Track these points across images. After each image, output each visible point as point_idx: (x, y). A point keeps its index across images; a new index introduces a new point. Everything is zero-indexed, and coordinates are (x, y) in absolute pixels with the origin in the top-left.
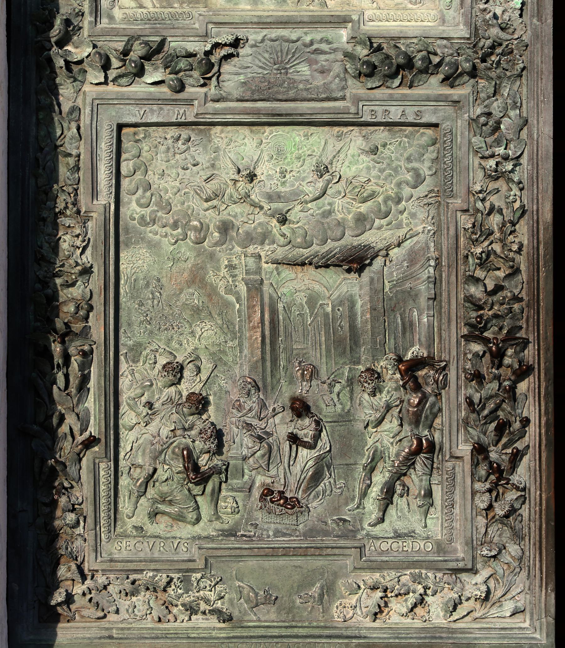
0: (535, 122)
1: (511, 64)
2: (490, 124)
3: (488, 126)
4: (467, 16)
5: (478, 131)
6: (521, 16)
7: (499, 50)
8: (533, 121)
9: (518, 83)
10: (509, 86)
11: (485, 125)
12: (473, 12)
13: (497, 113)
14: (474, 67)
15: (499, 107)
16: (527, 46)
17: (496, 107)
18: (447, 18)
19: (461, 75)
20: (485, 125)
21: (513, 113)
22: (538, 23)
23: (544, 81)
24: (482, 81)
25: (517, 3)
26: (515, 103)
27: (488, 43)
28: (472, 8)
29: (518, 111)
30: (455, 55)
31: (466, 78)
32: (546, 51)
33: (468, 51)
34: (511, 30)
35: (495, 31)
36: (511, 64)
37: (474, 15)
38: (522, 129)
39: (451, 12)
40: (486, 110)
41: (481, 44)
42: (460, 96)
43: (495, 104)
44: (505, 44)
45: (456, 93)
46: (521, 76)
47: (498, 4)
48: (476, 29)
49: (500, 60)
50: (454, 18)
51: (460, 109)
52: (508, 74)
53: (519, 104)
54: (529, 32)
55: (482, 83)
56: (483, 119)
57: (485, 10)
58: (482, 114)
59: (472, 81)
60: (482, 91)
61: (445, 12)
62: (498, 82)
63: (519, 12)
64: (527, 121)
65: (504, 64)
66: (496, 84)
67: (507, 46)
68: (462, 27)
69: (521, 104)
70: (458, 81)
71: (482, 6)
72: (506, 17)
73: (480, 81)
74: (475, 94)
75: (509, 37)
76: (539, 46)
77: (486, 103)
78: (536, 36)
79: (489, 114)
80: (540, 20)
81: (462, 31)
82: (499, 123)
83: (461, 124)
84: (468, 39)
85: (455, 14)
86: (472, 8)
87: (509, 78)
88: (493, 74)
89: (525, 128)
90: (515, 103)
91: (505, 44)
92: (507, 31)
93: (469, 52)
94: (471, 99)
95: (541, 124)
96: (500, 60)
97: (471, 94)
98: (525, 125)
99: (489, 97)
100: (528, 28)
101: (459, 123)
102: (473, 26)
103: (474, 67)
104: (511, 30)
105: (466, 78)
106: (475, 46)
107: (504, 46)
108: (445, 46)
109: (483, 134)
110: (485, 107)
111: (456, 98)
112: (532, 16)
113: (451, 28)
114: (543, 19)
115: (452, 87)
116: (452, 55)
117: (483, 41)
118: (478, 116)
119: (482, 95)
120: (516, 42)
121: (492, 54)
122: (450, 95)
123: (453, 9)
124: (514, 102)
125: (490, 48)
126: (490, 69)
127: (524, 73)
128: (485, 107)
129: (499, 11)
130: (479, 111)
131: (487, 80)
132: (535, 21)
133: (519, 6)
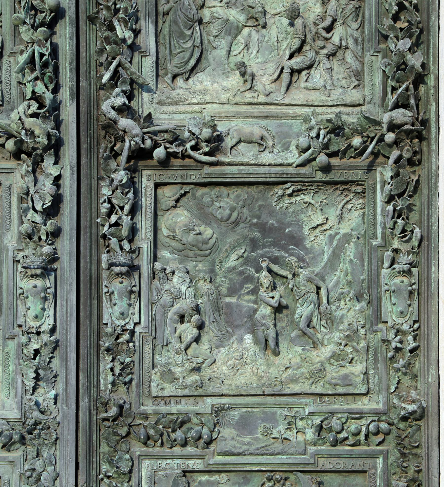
0: (64, 474)
1: (48, 436)
2: (34, 476)
3: (32, 478)
4: (18, 403)
5: (26, 481)
6: (55, 403)
7: (40, 427)
8: (62, 474)
9: (54, 448)
10: (47, 451)
11: (31, 476)
12: (23, 400)
13: (39, 468)
14: (23, 438)
15: (40, 465)
16: (59, 424)
17: (38, 465)
18: (6, 405)
19: (14, 443)
20: (31, 476)
21: (50, 469)
22: (66, 408)
23: (69, 447)
24: (29, 447)
25: (51, 395)
26: (51, 462)
27: (32, 422)
28: (22, 398)
29: (53, 468)
30: (10, 429)
31: (18, 445)
32: (71, 427)
33: (19, 427)
34: (49, 413)
35: (36, 414)
36: (48, 436)
37: (24, 403)
38: (56, 479)
39: (9, 401)
40: (32, 467)
41: (27, 422)
42: (14, 457)
43: (38, 463)
44: (43, 422)
45: (11, 455)
46: (56, 444)
47: (41, 395)
48: (25, 413)
49: (40, 433)
50: (11, 405)
51: (14, 466)
52: (46, 442)
53: (54, 463)
54: (60, 414)
55: (30, 448)
56: (28, 473)
57: (30, 399)
58: (28, 469)
59: (23, 447)
60: (29, 454)
61: (5, 401)
62: (39, 448)
63: (54, 401)
64: (59, 474)
65: (43, 436)
66: (38, 449)
67: (45, 423)
68: (16, 411)
69: (56, 462)
70: (13, 447)
71: (29, 397)
72: (45, 404)
73: (28, 447)
74: (25, 456)
75: (46, 417)
76: (66, 423)
77: (31, 462)
78: (65, 417)
79: (34, 470)
80: (67, 406)
81: (14, 414)
82: (40, 475)
83: (15, 477)
84: (20, 419)
85: (12, 402)
86: (22, 398)
87: (47, 445)
88: (36, 442)
89: (58, 479)
90: (51, 462)
91: (43, 422)
92: (46, 414)
93: (20, 428)
94: (22, 459)
95: (67, 476)
96: (40, 433)
97: (22, 456)
98: (58, 477)
99: (34, 458)
100: (60, 411)
101: (14, 477)
102: (23, 410)
103: (23, 438)
104: (49, 413)
105: (18, 445)
106: (24, 424)
107: (43, 424)
108: (3, 424)
109: (29, 483)
110: (31, 464)
111: (11, 459)
112: (62, 404)
113: (8, 412)
114: (69, 405)
115: (9, 451)
116: (8, 430)
117: (29, 420)
118: (26, 471)
119: (29, 457)
120: (51, 420)
121: (35, 429)
122: (7, 457)
123: (10, 399)
124: (50, 461)
125: (34, 425)
126: (34, 439)
127: (58, 441)
128: (31, 464)
129: (40, 400)
130: (27, 467)
131: (32, 447)
132: (64, 406)
133: (53, 397)
